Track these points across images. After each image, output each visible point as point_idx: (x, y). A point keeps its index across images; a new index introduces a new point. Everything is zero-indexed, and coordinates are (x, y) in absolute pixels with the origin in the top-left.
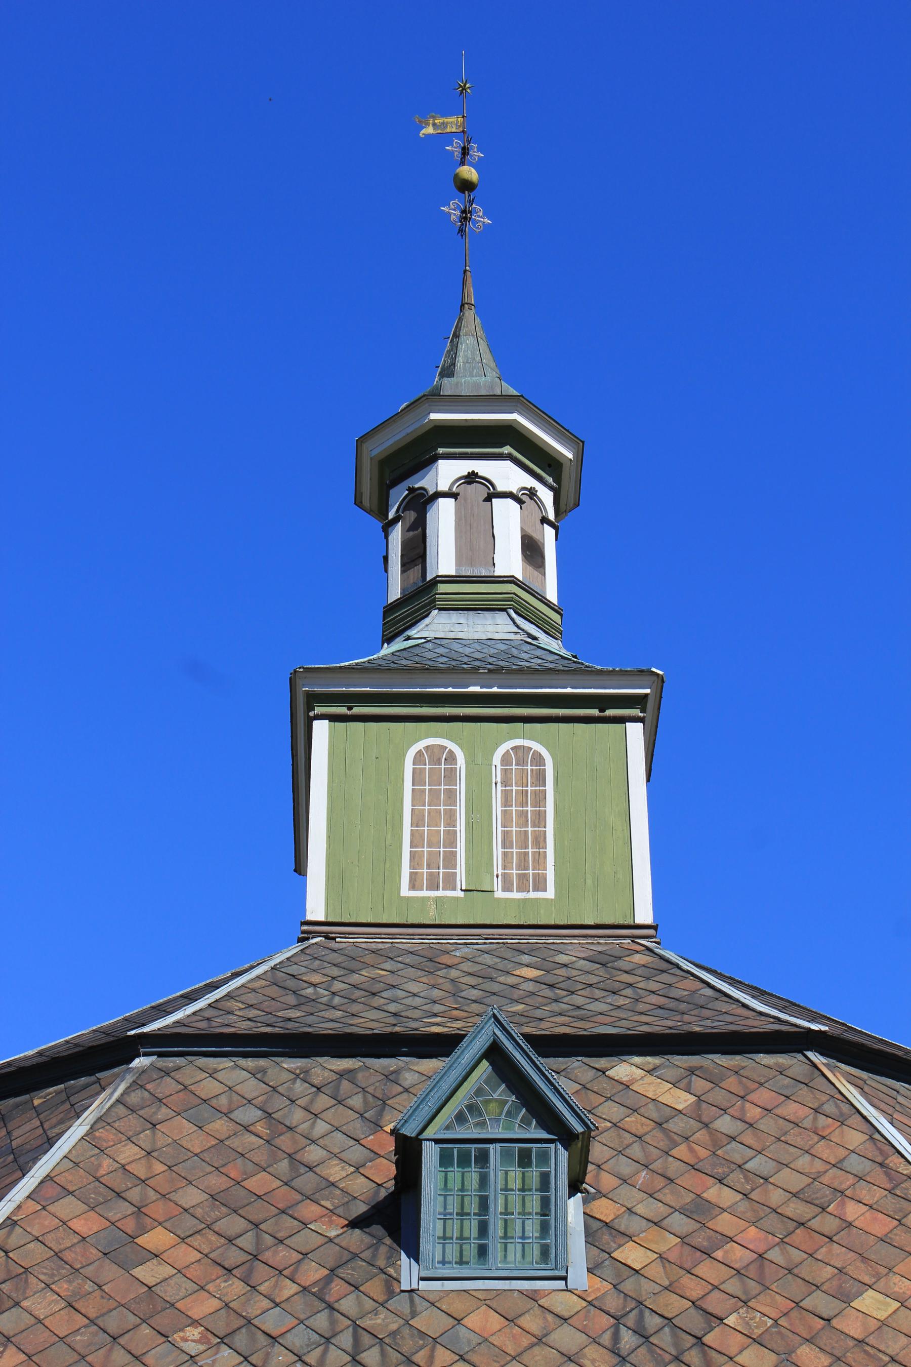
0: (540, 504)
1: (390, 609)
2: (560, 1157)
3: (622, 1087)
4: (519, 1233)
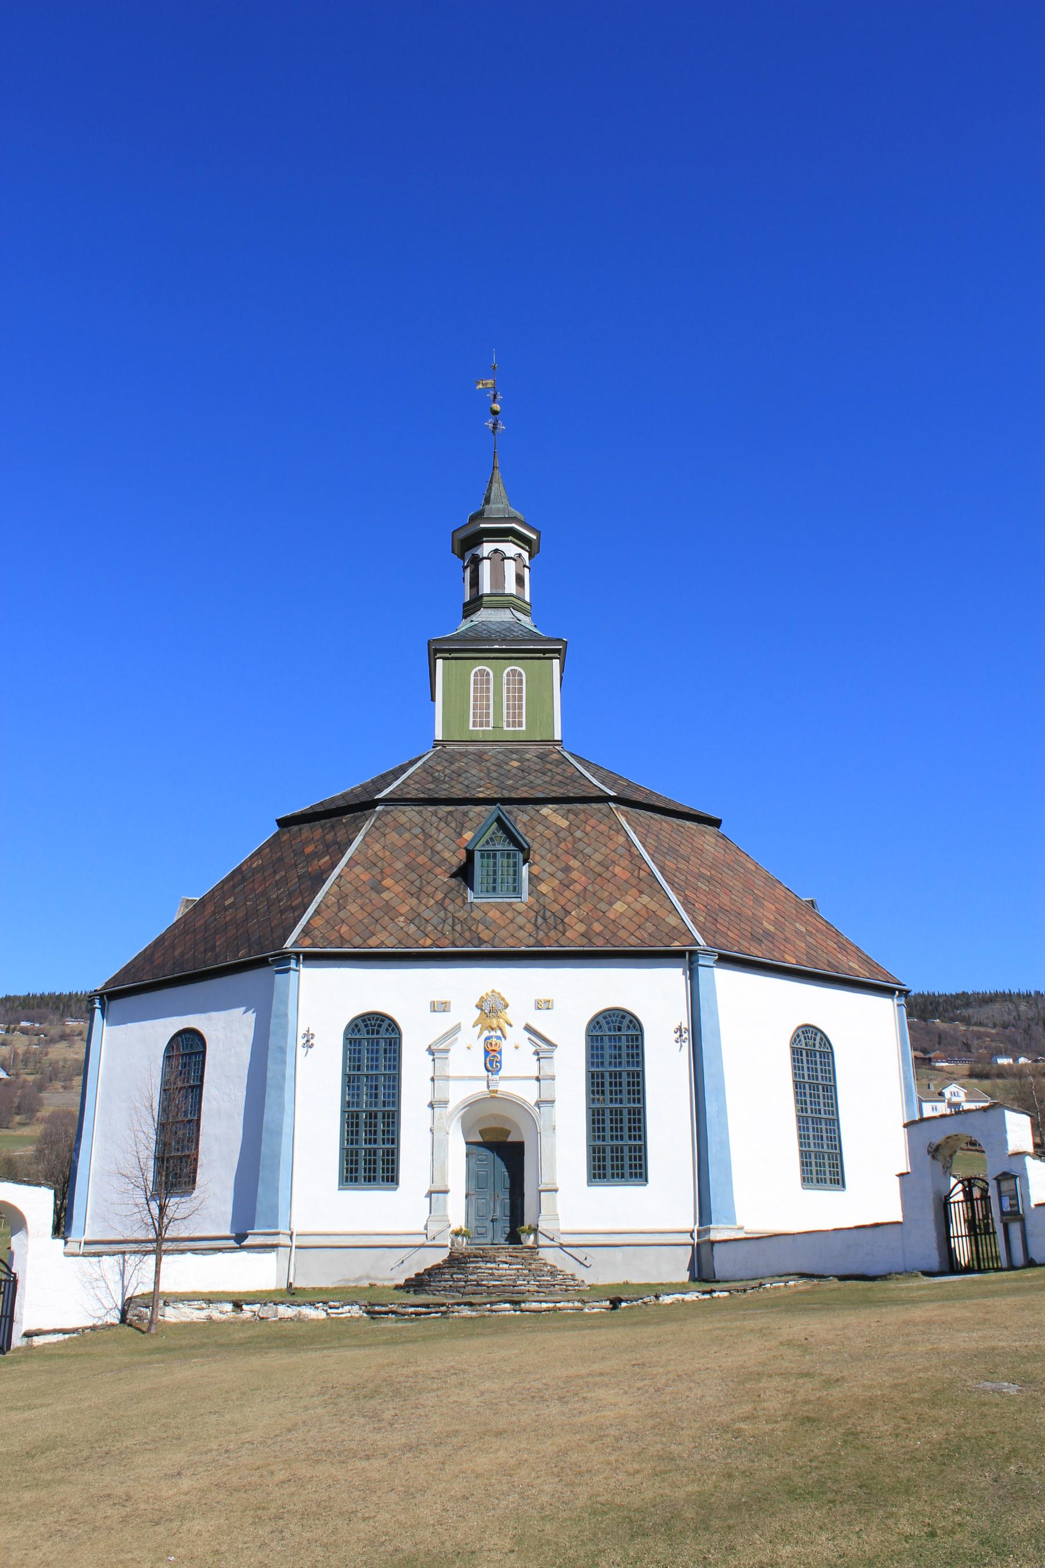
0: (523, 560)
1: (465, 605)
2: (520, 856)
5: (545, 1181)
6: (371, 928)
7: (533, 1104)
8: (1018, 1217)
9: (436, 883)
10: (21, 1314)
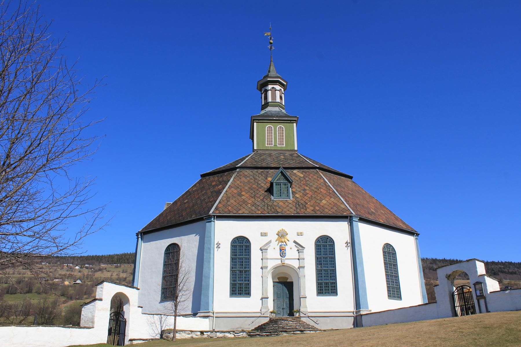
0: (282, 91)
1: (262, 106)
2: (289, 185)
5: (302, 294)
6: (239, 208)
7: (297, 268)
8: (483, 297)
9: (260, 193)
10: (128, 333)
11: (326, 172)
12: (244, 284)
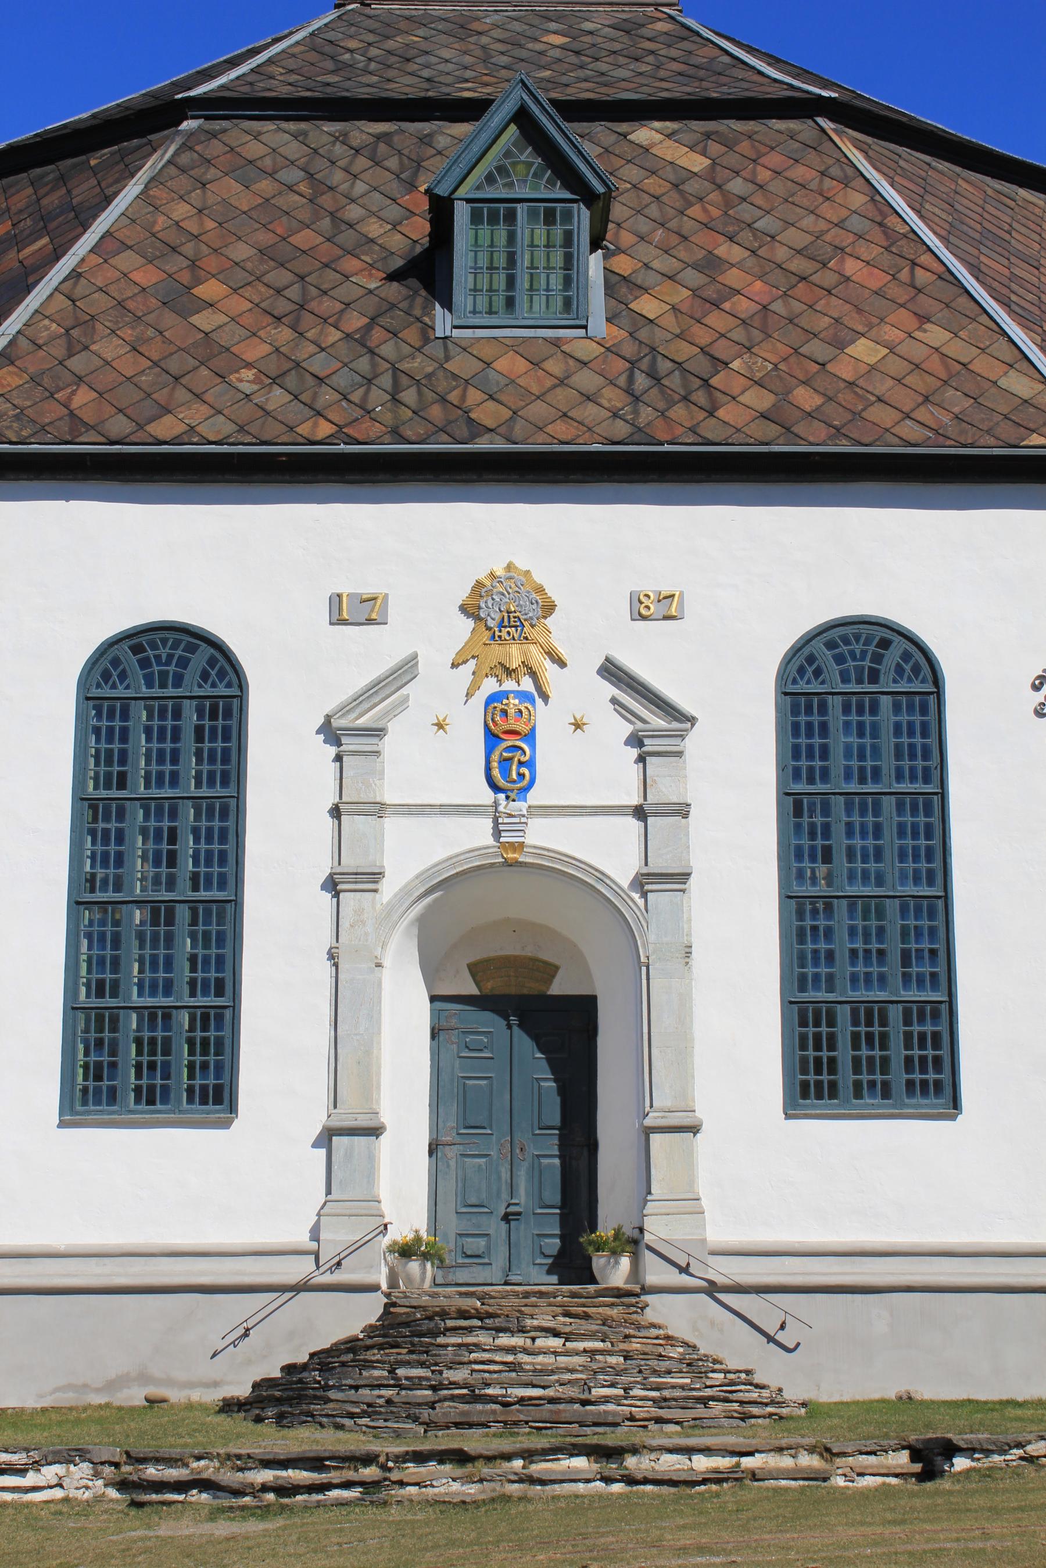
3: (641, 150)
4: (543, 286)
6: (161, 396)
7: (625, 884)
11: (892, 146)
12: (185, 1018)
